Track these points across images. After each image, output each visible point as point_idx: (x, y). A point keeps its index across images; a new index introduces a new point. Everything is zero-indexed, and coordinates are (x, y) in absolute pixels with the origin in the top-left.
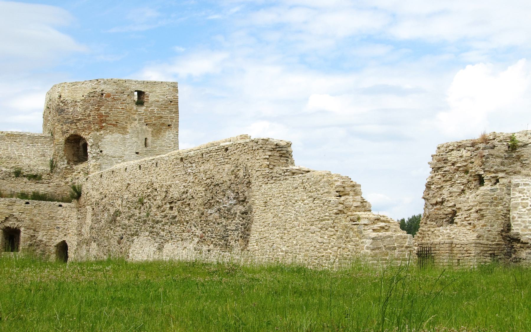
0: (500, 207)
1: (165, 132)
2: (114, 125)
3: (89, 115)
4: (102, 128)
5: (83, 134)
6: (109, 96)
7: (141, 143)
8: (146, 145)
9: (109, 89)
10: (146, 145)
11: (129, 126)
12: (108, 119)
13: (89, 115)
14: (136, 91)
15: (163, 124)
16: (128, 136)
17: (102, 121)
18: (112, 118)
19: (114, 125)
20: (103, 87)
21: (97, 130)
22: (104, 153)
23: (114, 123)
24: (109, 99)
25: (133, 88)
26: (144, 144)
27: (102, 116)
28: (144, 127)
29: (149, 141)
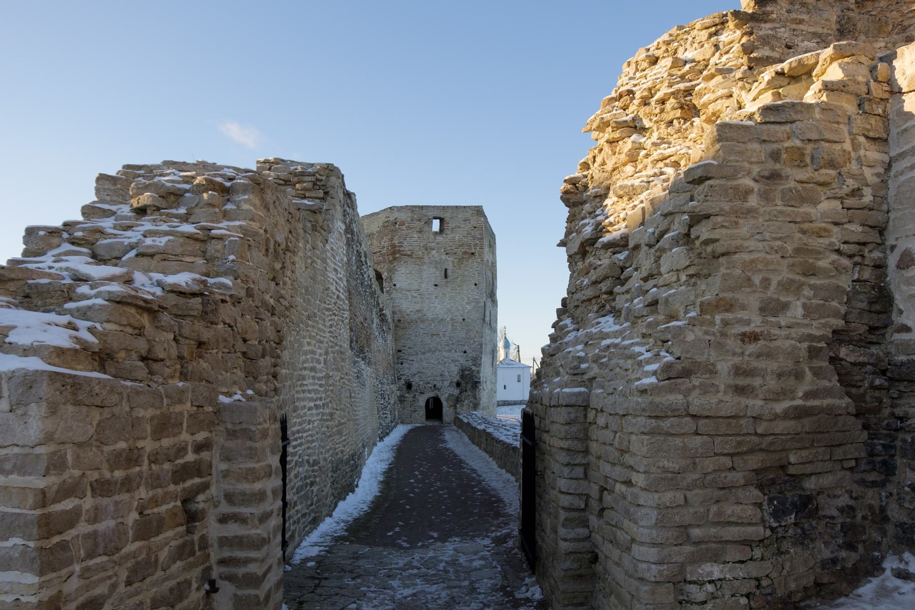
0: (826, 206)
1: (467, 261)
2: (409, 256)
3: (384, 247)
4: (395, 259)
6: (402, 224)
7: (439, 274)
8: (446, 277)
9: (402, 216)
10: (446, 277)
11: (426, 257)
12: (401, 249)
13: (384, 247)
14: (435, 218)
15: (465, 253)
16: (425, 267)
17: (394, 253)
18: (406, 248)
19: (409, 256)
20: (396, 214)
21: (391, 262)
22: (397, 286)
23: (409, 253)
24: (404, 228)
25: (431, 214)
26: (443, 275)
27: (394, 246)
28: (443, 257)
29: (449, 272)
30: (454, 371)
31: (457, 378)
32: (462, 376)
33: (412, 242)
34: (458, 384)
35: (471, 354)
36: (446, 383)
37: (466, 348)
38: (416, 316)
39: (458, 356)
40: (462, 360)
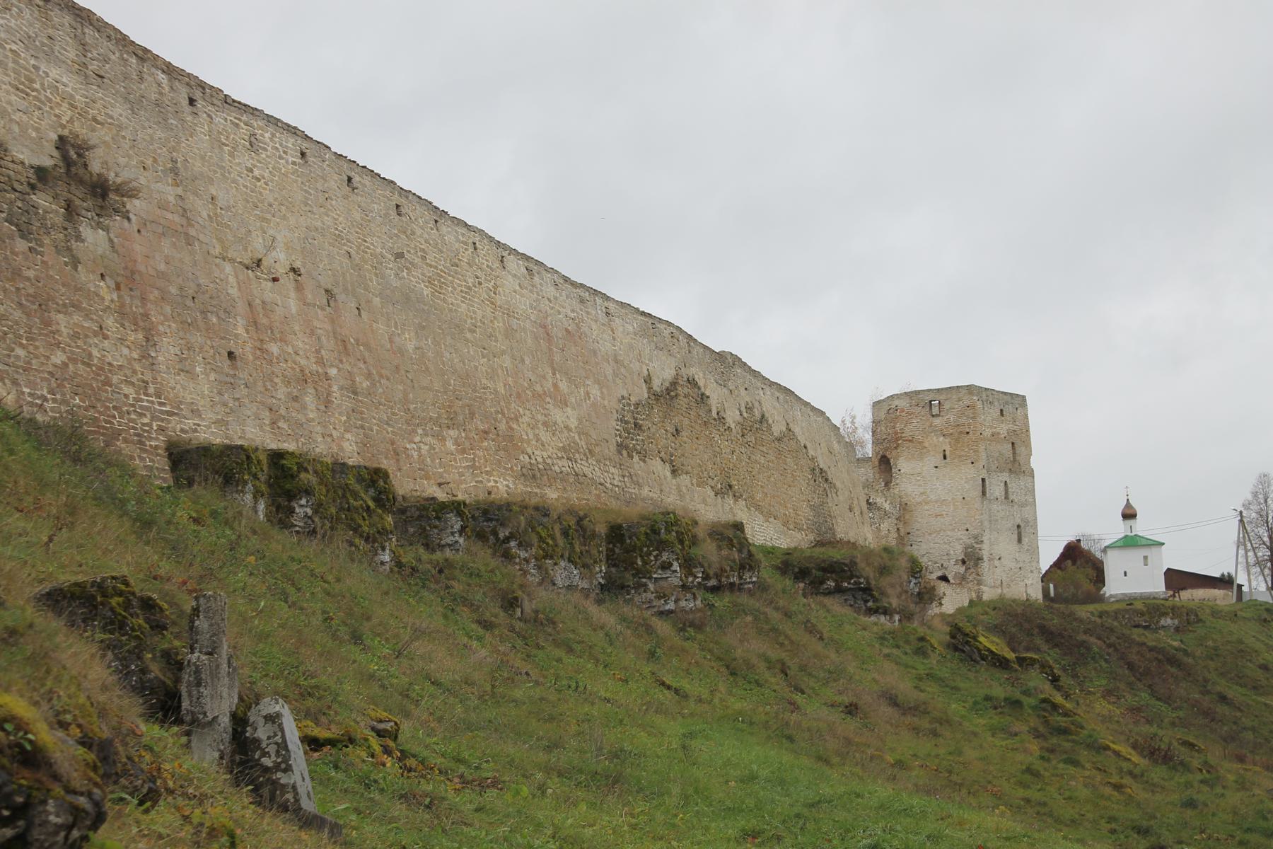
5: (887, 454)
8: (945, 457)
9: (902, 404)
10: (945, 457)
17: (897, 439)
20: (897, 402)
27: (896, 433)
29: (947, 453)
30: (959, 553)
31: (962, 556)
32: (966, 555)
33: (912, 428)
34: (964, 562)
35: (973, 531)
36: (952, 562)
37: (968, 526)
38: (919, 500)
39: (961, 534)
40: (965, 539)
